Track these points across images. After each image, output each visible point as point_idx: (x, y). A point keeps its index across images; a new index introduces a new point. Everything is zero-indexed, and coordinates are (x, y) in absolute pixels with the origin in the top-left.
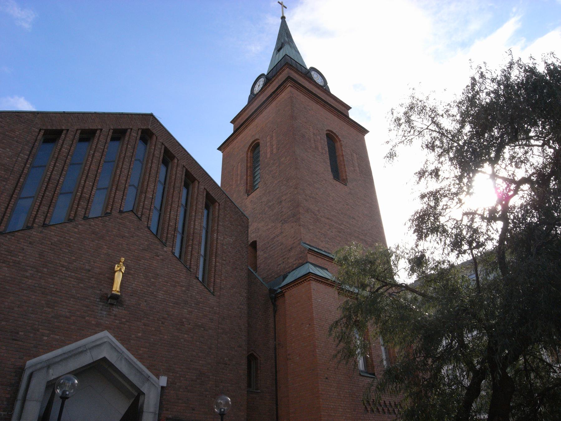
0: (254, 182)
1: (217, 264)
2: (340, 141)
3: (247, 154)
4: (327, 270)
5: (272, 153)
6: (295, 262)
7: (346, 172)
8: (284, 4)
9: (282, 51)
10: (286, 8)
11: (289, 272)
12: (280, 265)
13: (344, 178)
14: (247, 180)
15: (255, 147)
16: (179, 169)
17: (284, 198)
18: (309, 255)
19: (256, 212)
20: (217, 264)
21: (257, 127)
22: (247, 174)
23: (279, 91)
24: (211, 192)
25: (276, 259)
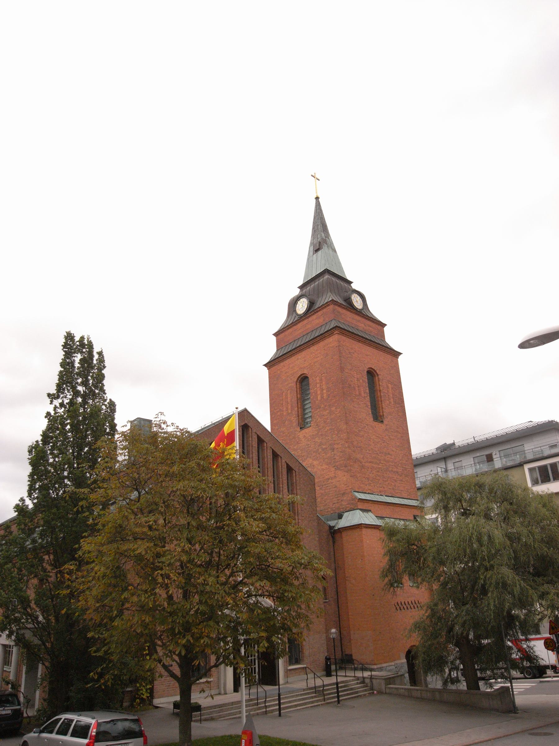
0: (305, 414)
1: (300, 521)
2: (378, 375)
3: (296, 384)
4: (370, 511)
5: (322, 397)
6: (347, 506)
7: (382, 408)
8: (317, 176)
9: (320, 253)
10: (319, 180)
11: (344, 513)
12: (334, 503)
13: (381, 414)
14: (298, 412)
15: (303, 380)
16: (268, 451)
17: (336, 446)
18: (359, 503)
19: (310, 448)
20: (300, 521)
21: (305, 361)
22: (298, 406)
23: (326, 335)
24: (289, 464)
25: (332, 497)
